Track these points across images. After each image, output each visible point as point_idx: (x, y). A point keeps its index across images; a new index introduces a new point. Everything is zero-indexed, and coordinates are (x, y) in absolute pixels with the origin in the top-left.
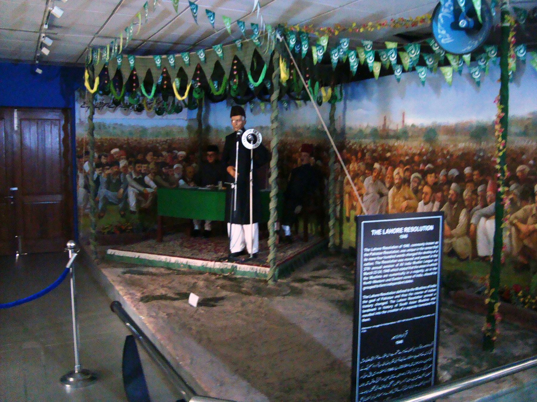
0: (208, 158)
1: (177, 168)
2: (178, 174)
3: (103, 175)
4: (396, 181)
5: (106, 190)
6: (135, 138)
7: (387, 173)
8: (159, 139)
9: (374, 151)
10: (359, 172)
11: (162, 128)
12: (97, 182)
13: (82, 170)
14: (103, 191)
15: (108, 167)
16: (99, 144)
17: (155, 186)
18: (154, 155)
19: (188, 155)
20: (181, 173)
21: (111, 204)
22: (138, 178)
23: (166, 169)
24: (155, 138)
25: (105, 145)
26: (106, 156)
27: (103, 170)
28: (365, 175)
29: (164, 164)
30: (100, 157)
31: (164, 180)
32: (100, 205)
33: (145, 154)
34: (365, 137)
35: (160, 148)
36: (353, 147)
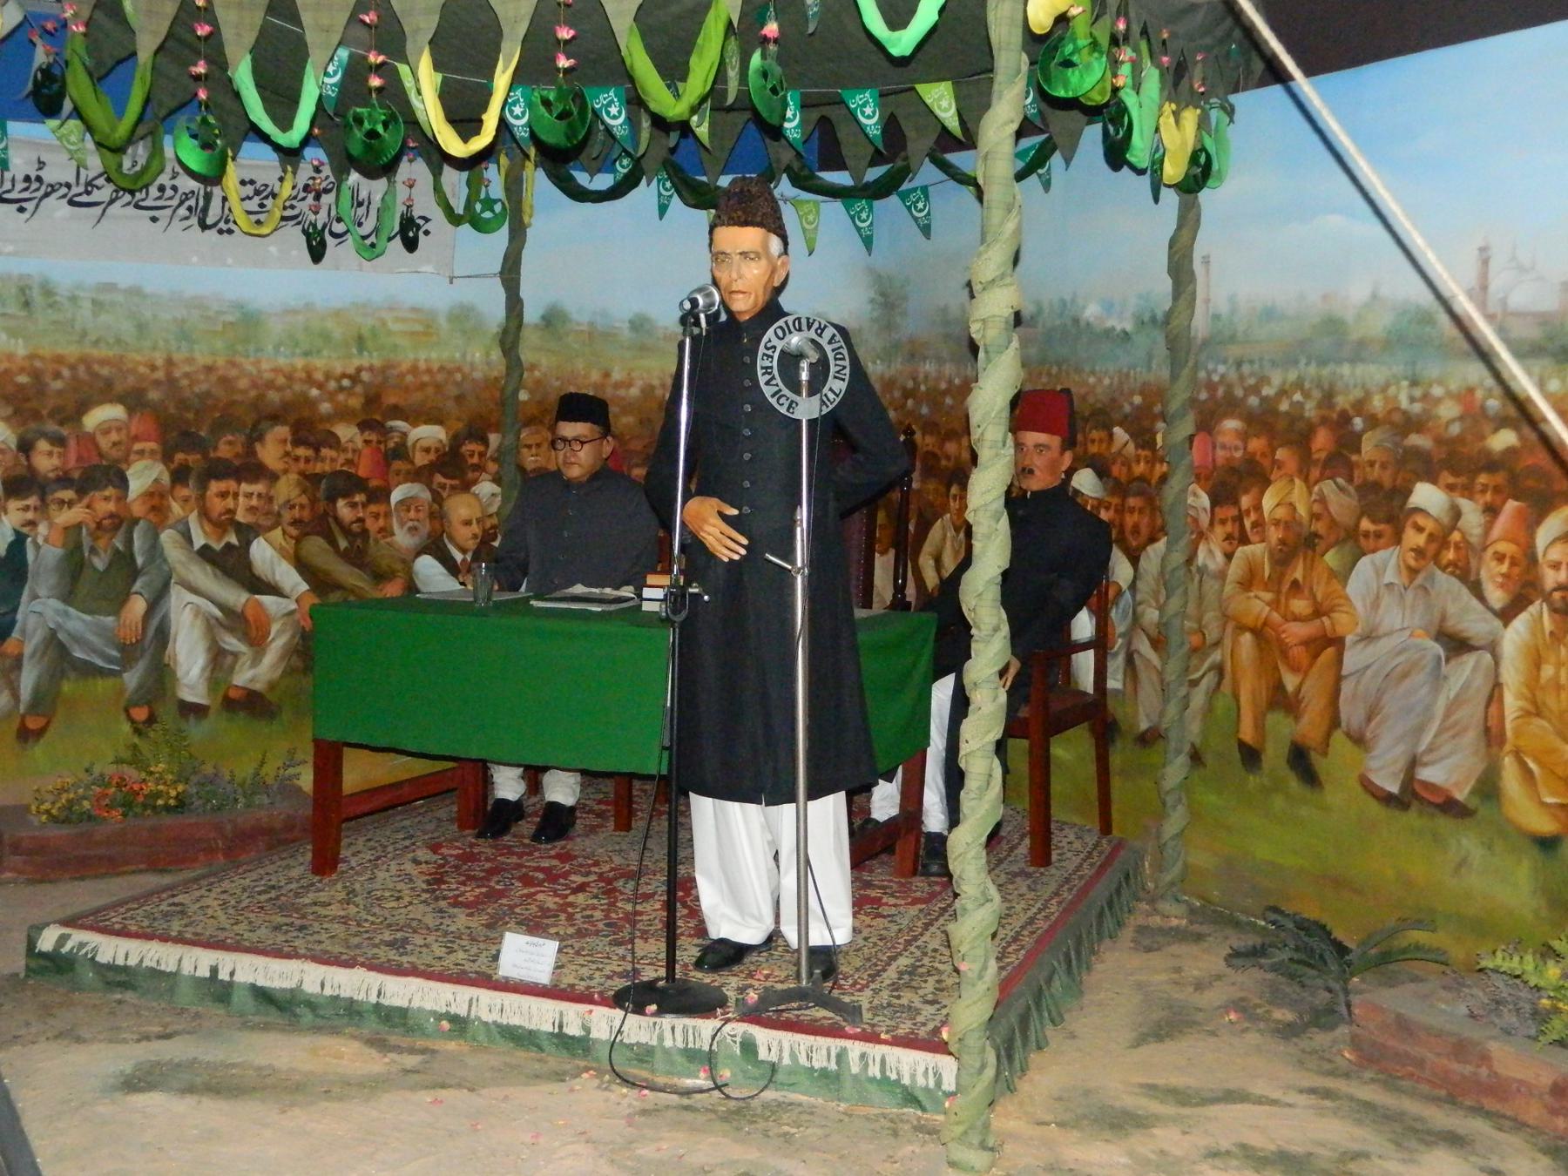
1: (405, 504)
2: (413, 530)
3: (42, 529)
5: (55, 604)
6: (202, 359)
7: (1497, 531)
8: (319, 363)
9: (1411, 424)
10: (1319, 527)
11: (337, 314)
15: (68, 494)
16: (23, 379)
17: (304, 587)
19: (456, 441)
20: (425, 528)
21: (88, 671)
22: (218, 546)
23: (353, 505)
24: (300, 363)
25: (58, 385)
26: (59, 441)
27: (43, 507)
28: (1355, 544)
30: (25, 447)
31: (346, 556)
32: (28, 679)
34: (1359, 352)
35: (325, 407)
36: (1284, 406)
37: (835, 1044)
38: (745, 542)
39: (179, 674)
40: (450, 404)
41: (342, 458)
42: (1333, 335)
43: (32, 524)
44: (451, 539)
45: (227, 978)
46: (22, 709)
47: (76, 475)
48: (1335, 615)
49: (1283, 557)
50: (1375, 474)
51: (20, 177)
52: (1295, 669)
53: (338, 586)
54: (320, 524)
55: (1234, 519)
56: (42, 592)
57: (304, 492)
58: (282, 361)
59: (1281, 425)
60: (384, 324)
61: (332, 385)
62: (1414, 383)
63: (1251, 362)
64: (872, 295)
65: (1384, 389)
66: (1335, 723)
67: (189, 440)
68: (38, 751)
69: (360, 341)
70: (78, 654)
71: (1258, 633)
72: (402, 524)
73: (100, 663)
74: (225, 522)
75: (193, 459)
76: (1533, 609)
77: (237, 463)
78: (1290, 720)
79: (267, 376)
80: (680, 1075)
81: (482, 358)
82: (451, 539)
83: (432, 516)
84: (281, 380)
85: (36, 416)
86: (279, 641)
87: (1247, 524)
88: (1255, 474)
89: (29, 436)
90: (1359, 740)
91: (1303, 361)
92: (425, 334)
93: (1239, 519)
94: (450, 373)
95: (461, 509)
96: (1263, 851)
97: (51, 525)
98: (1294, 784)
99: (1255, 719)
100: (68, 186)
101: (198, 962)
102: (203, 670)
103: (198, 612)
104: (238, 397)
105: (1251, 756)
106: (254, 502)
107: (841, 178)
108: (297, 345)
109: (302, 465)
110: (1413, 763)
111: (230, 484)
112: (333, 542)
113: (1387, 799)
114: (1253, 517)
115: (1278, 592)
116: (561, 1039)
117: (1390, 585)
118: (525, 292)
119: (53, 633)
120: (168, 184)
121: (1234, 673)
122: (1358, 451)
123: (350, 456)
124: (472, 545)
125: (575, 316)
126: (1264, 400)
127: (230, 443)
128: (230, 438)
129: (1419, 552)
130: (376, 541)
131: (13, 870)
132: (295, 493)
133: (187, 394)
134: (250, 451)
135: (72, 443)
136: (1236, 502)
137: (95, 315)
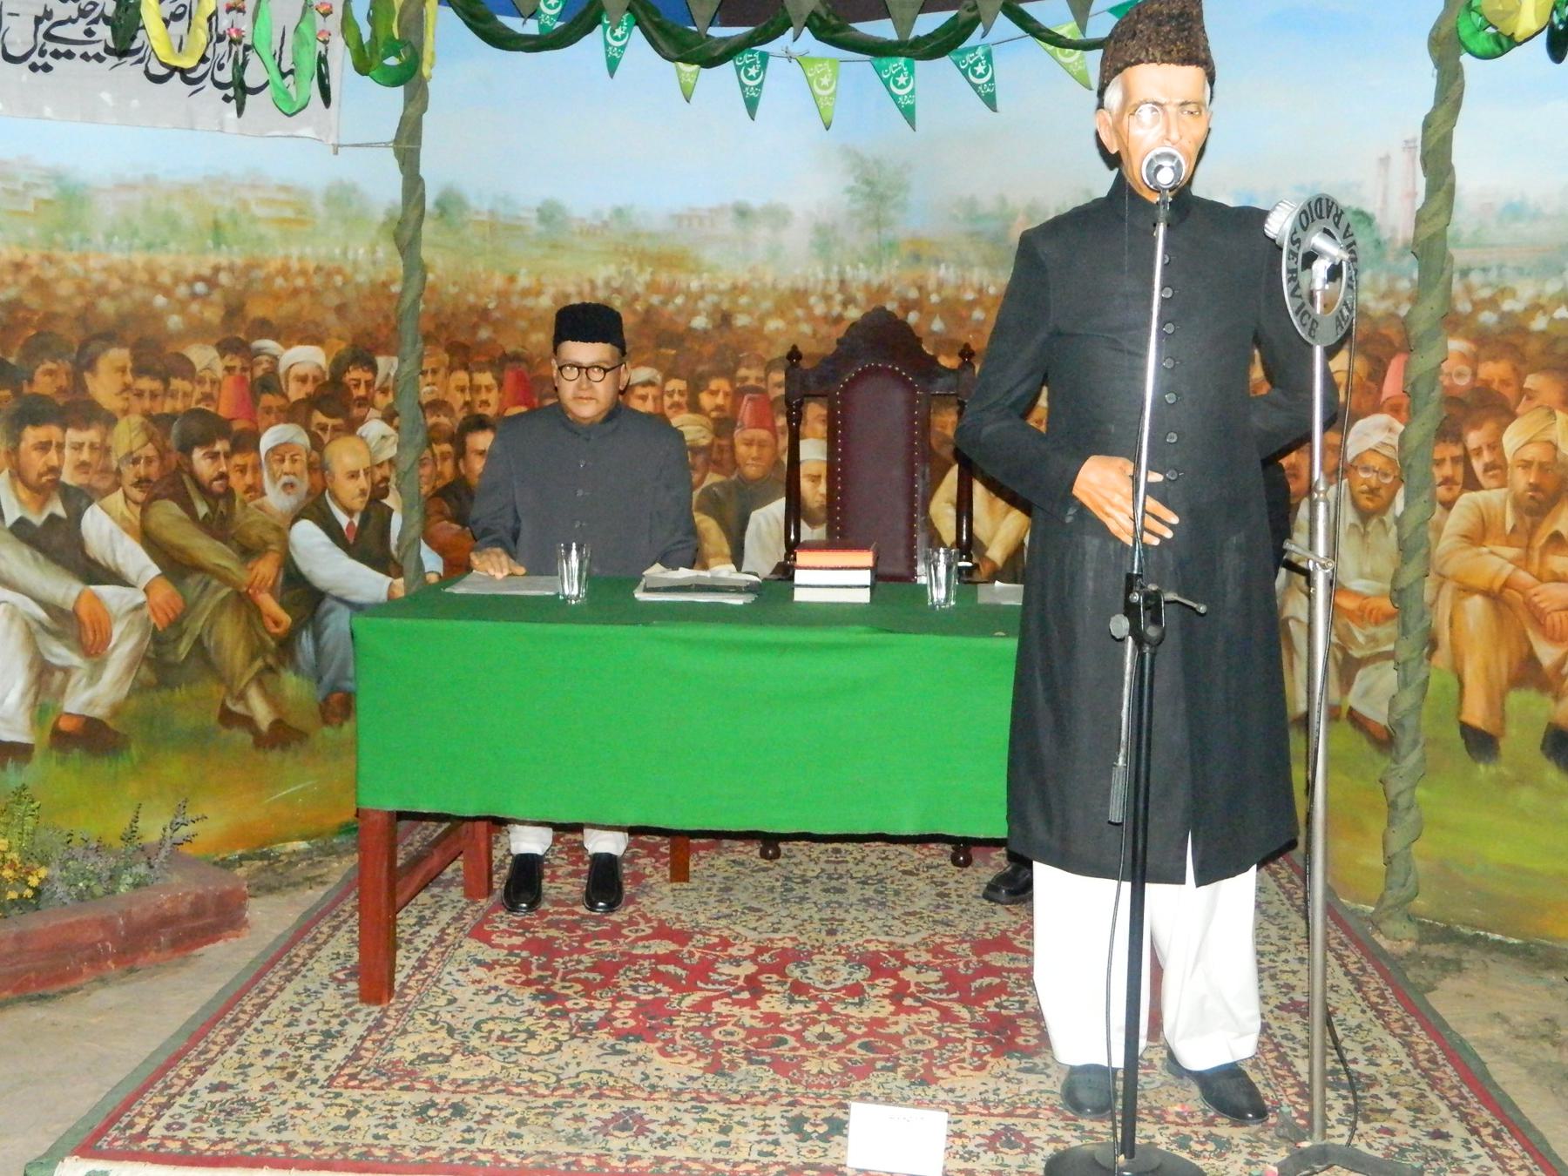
0: (569, 387)
1: (278, 452)
2: (289, 486)
8: (164, 259)
11: (188, 191)
17: (154, 570)
19: (339, 366)
20: (303, 485)
22: (38, 520)
23: (214, 456)
24: (139, 259)
29: (204, 427)
33: (85, 363)
35: (175, 322)
36: (1539, 323)
38: (1175, 520)
40: (331, 319)
44: (335, 497)
49: (1537, 506)
52: (1554, 638)
53: (198, 568)
54: (173, 483)
55: (1454, 460)
57: (151, 439)
58: (117, 256)
59: (1533, 347)
60: (245, 204)
61: (182, 291)
63: (1485, 270)
64: (851, 182)
71: (1496, 597)
72: (274, 479)
74: (46, 486)
77: (61, 401)
78: (1548, 700)
79: (98, 277)
81: (368, 258)
82: (335, 497)
83: (311, 467)
84: (115, 284)
86: (124, 645)
87: (1478, 465)
88: (1492, 405)
92: (302, 223)
93: (1466, 459)
94: (329, 275)
95: (345, 456)
96: (1499, 852)
102: (24, 695)
103: (13, 612)
104: (59, 308)
105: (1481, 743)
106: (85, 455)
107: (882, 29)
108: (135, 233)
109: (147, 403)
111: (50, 432)
112: (188, 507)
114: (1487, 457)
115: (1528, 547)
118: (424, 171)
121: (1454, 645)
123: (207, 388)
124: (359, 504)
125: (473, 202)
126: (1505, 316)
127: (50, 373)
128: (50, 365)
132: (140, 439)
134: (79, 384)
136: (1458, 438)
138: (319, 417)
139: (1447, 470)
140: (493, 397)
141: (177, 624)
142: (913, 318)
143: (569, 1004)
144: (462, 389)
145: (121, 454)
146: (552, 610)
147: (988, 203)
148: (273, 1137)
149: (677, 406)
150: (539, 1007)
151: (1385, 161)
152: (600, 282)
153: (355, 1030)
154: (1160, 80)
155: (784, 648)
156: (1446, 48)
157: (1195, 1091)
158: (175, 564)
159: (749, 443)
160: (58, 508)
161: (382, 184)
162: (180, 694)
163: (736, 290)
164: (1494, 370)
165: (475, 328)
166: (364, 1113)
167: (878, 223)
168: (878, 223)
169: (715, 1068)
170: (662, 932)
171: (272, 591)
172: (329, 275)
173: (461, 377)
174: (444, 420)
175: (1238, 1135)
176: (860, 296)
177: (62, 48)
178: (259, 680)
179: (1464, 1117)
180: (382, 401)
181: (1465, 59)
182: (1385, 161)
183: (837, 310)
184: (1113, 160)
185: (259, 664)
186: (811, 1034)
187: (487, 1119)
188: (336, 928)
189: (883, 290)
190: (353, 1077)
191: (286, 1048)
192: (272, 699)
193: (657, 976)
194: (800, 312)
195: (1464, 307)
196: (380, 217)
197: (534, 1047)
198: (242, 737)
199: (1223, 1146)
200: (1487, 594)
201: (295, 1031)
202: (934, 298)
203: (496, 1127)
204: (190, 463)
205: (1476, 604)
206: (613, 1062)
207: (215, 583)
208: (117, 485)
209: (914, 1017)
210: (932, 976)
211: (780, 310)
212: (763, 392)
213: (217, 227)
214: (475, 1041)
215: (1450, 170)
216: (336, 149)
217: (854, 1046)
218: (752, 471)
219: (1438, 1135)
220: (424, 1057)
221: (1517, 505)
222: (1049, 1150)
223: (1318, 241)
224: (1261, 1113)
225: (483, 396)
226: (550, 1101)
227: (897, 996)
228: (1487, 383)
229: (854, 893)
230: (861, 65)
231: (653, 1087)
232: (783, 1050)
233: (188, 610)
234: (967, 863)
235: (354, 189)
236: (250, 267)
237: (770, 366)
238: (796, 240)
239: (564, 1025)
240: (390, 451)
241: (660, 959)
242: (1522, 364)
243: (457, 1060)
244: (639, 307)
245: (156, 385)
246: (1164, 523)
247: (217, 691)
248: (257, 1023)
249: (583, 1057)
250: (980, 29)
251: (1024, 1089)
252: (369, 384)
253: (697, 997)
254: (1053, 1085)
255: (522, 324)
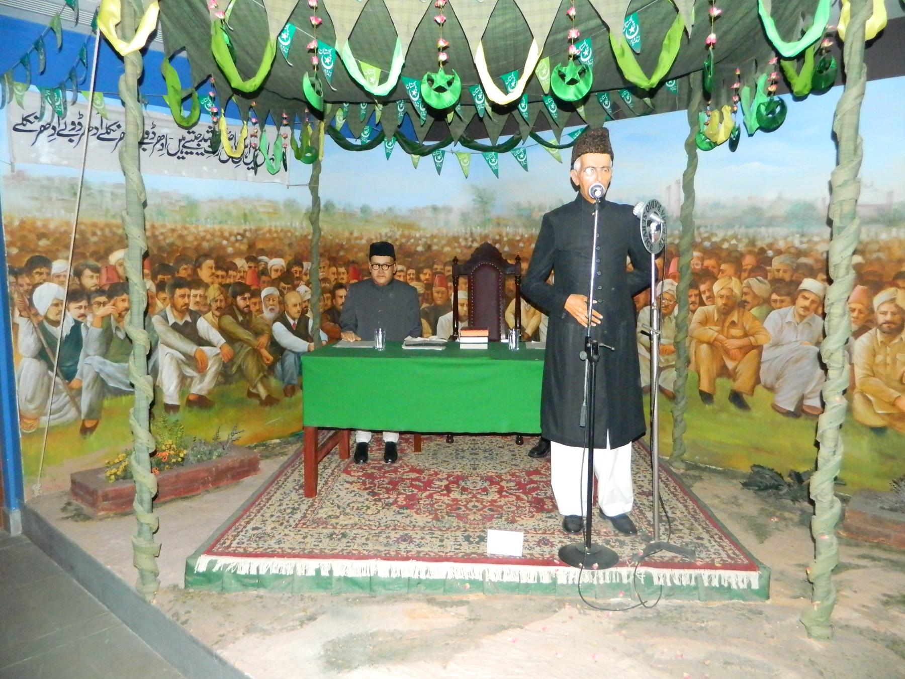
0: (375, 273)
1: (268, 297)
2: (272, 310)
3: (89, 318)
4: (881, 319)
5: (99, 359)
6: (170, 225)
8: (226, 228)
9: (800, 253)
10: (748, 298)
11: (234, 202)
12: (75, 339)
13: (29, 308)
14: (90, 362)
15: (103, 299)
17: (223, 341)
18: (218, 268)
19: (290, 266)
20: (277, 309)
22: (181, 323)
23: (245, 299)
24: (217, 227)
25: (94, 239)
26: (97, 270)
28: (768, 304)
29: (241, 288)
30: (78, 273)
31: (242, 324)
33: (198, 265)
34: (771, 222)
35: (230, 250)
36: (725, 246)
37: (694, 572)
38: (601, 317)
39: (164, 390)
40: (286, 248)
41: (239, 275)
42: (756, 215)
43: (84, 316)
45: (327, 574)
46: (83, 417)
47: (106, 288)
48: (757, 336)
49: (726, 311)
50: (781, 275)
51: (69, 122)
52: (733, 359)
53: (240, 340)
54: (229, 309)
55: (696, 295)
56: (91, 352)
57: (222, 293)
58: (209, 226)
59: (724, 254)
60: (255, 208)
61: (233, 239)
62: (803, 235)
63: (706, 227)
64: (474, 197)
65: (786, 238)
66: (758, 381)
67: (165, 268)
68: (92, 438)
69: (245, 217)
70: (112, 384)
71: (711, 344)
72: (267, 307)
73: (123, 388)
74: (184, 310)
75: (167, 278)
76: (872, 332)
77: (189, 279)
78: (731, 381)
79: (202, 234)
80: (610, 598)
81: (300, 226)
83: (280, 303)
84: (209, 237)
85: (83, 255)
86: (212, 368)
87: (704, 297)
88: (709, 276)
89: (81, 267)
90: (771, 389)
91: (737, 226)
92: (275, 213)
93: (700, 295)
94: (286, 233)
95: (292, 299)
96: (713, 437)
97: (94, 316)
98: (733, 408)
99: (710, 381)
100: (97, 128)
101: (308, 567)
102: (176, 387)
103: (172, 357)
104: (188, 245)
105: (707, 397)
106: (198, 299)
107: (486, 142)
108: (215, 218)
110: (802, 398)
112: (236, 318)
113: (788, 414)
114: (707, 294)
115: (723, 326)
116: (539, 587)
117: (789, 323)
119: (98, 375)
120: (151, 131)
121: (696, 362)
122: (771, 265)
124: (297, 316)
125: (337, 205)
126: (713, 243)
127: (185, 269)
128: (185, 266)
129: (806, 308)
130: (256, 316)
131: (103, 510)
133: (163, 243)
134: (195, 272)
135: (104, 271)
136: (697, 288)
137: (113, 200)
138: (282, 284)
139: (693, 299)
140: (345, 276)
141: (232, 361)
142: (497, 246)
143: (381, 496)
144: (334, 274)
145: (211, 297)
146: (373, 353)
147: (524, 204)
148: (277, 546)
149: (412, 279)
150: (370, 498)
151: (669, 188)
152: (383, 234)
153: (304, 507)
154: (594, 159)
155: (460, 365)
156: (691, 147)
157: (610, 523)
158: (231, 338)
159: (438, 292)
160: (188, 319)
161: (305, 200)
162: (233, 386)
163: (433, 237)
164: (709, 263)
165: (338, 251)
166: (309, 537)
167: (484, 212)
168: (484, 212)
169: (436, 518)
170: (413, 470)
171: (266, 349)
172: (286, 233)
173: (334, 269)
174: (328, 285)
175: (627, 539)
176: (478, 238)
177: (189, 151)
178: (261, 380)
179: (708, 532)
180: (305, 278)
181: (698, 151)
182: (669, 188)
183: (470, 244)
184: (577, 188)
185: (261, 375)
186: (470, 505)
187: (354, 538)
188: (294, 470)
189: (486, 236)
190: (304, 524)
191: (279, 514)
192: (267, 387)
193: (412, 485)
194: (456, 244)
195: (698, 240)
196: (304, 211)
197: (369, 512)
198: (256, 402)
199: (622, 544)
200: (708, 343)
201: (282, 508)
202: (505, 239)
203: (358, 541)
204: (236, 302)
205: (704, 347)
206: (399, 517)
207: (245, 345)
208: (210, 310)
209: (507, 499)
210: (512, 484)
211: (449, 244)
212: (443, 274)
213: (245, 215)
214: (348, 510)
215: (693, 191)
216: (288, 187)
217: (486, 510)
218: (439, 302)
219: (699, 538)
220: (330, 516)
221: (719, 311)
222: (559, 546)
223: (652, 216)
224: (635, 531)
225: (342, 276)
226: (377, 532)
227: (500, 491)
228: (707, 267)
229: (481, 455)
230: (479, 155)
231: (414, 526)
232: (460, 512)
233: (236, 355)
234: (522, 443)
235: (294, 201)
236: (256, 230)
237: (445, 264)
238: (454, 218)
239: (380, 504)
240: (308, 297)
241: (413, 480)
242: (720, 260)
243: (342, 517)
244: (398, 243)
245: (223, 273)
246: (598, 318)
247: (247, 385)
248: (268, 505)
249: (388, 515)
250: (522, 141)
251: (549, 524)
252: (301, 272)
253: (427, 493)
254: (559, 522)
255: (356, 250)
